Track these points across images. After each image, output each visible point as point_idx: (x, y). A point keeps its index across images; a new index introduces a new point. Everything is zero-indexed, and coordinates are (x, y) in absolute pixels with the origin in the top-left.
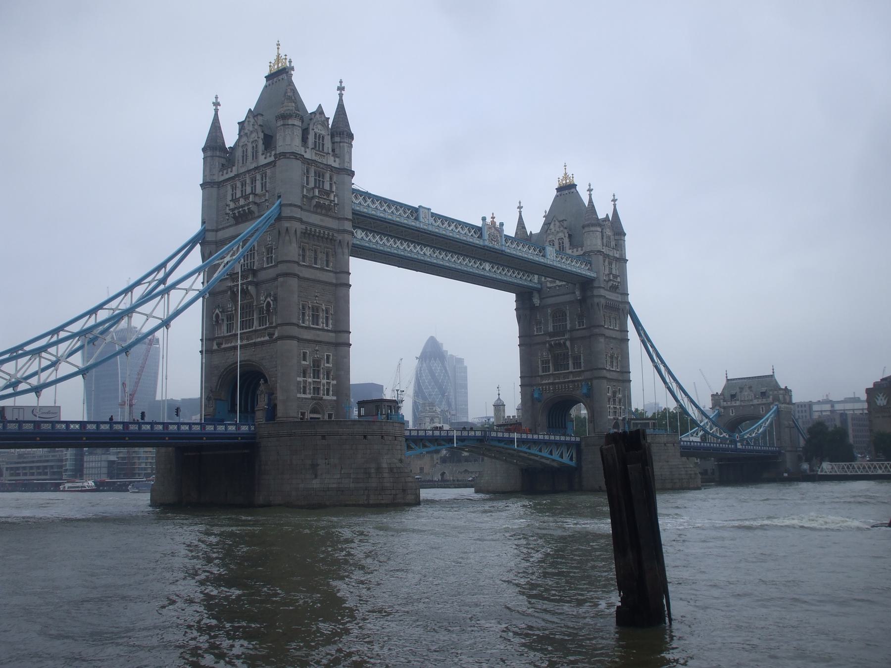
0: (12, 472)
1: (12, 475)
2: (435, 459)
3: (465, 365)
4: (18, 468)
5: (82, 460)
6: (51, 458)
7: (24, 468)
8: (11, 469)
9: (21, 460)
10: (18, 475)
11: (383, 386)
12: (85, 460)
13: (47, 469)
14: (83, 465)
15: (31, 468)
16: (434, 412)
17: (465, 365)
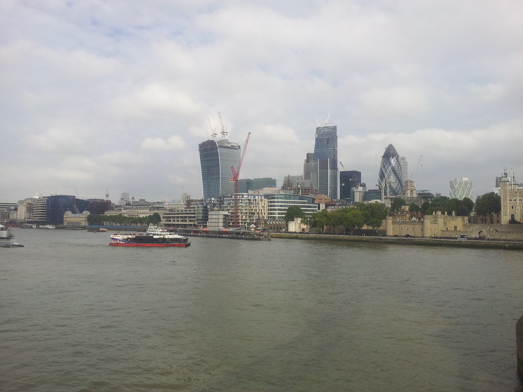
0: (166, 219)
1: (167, 221)
2: (465, 221)
3: (406, 161)
4: (170, 217)
5: (207, 214)
6: (188, 212)
7: (174, 217)
8: (166, 217)
9: (170, 213)
10: (170, 221)
11: (361, 172)
12: (209, 214)
13: (186, 218)
14: (207, 217)
15: (178, 217)
16: (413, 187)
17: (406, 161)
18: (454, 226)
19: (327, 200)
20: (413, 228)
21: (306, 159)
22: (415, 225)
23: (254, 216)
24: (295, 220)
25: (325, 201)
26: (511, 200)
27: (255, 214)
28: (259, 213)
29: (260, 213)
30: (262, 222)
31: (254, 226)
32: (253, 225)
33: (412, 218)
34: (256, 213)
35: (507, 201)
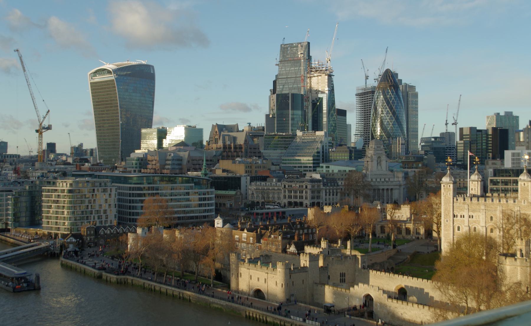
18: (341, 274)
19: (260, 168)
20: (265, 280)
22: (268, 273)
23: (91, 216)
25: (257, 169)
26: (457, 215)
27: (92, 214)
28: (100, 210)
29: (102, 212)
30: (90, 232)
31: (74, 240)
32: (71, 238)
33: (290, 247)
34: (94, 212)
35: (450, 217)
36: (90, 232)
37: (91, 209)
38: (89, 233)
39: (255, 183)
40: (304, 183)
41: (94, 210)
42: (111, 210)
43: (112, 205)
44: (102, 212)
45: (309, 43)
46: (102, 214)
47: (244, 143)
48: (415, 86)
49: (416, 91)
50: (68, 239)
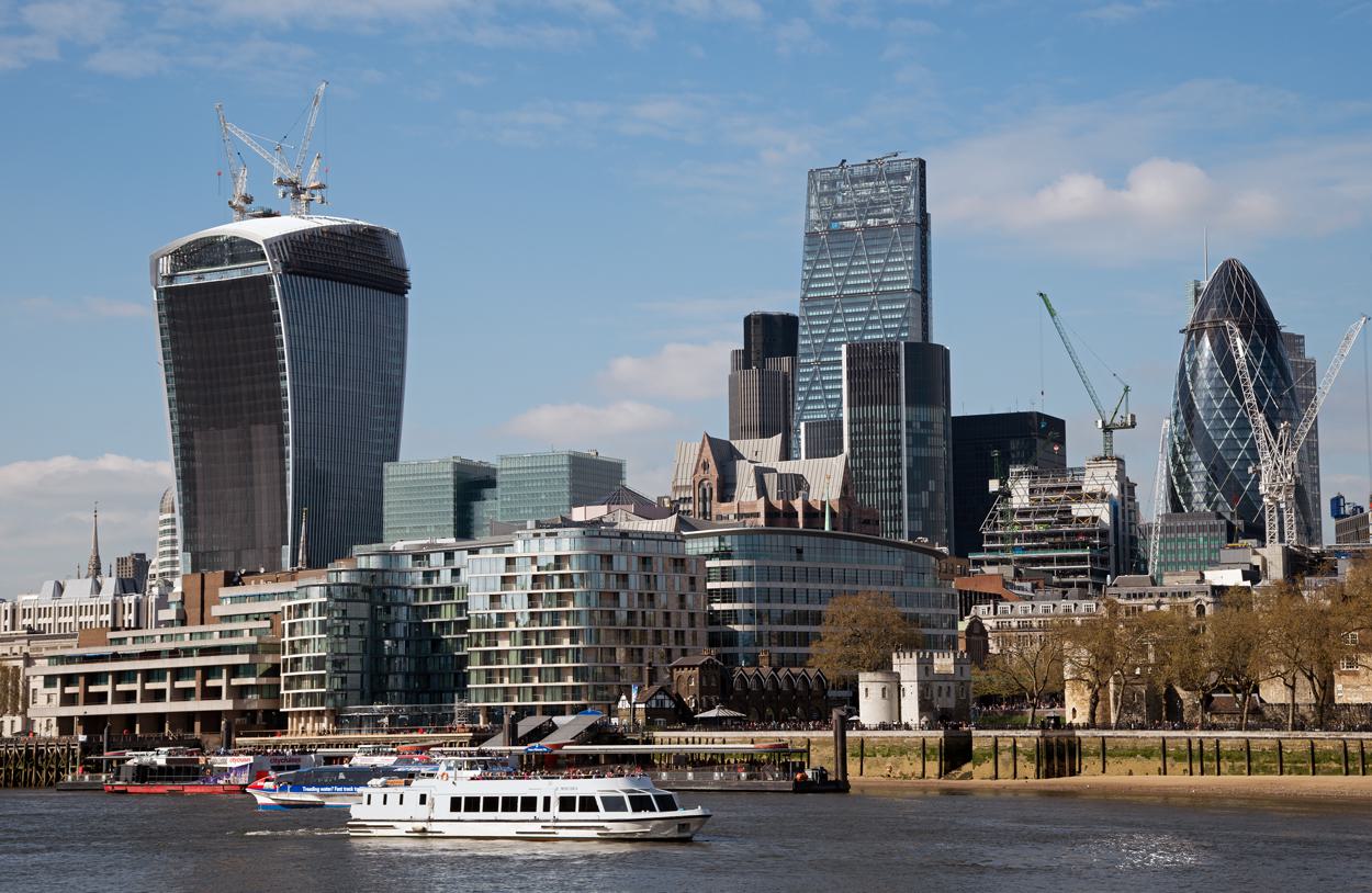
21: (742, 347)
23: (641, 650)
24: (896, 669)
30: (709, 682)
31: (668, 704)
32: (660, 697)
36: (709, 682)
37: (644, 625)
38: (704, 684)
39: (992, 606)
40: (1192, 599)
41: (650, 629)
42: (694, 635)
43: (697, 619)
44: (672, 637)
45: (922, 164)
46: (672, 645)
47: (842, 499)
48: (1302, 337)
49: (1308, 355)
50: (650, 699)
